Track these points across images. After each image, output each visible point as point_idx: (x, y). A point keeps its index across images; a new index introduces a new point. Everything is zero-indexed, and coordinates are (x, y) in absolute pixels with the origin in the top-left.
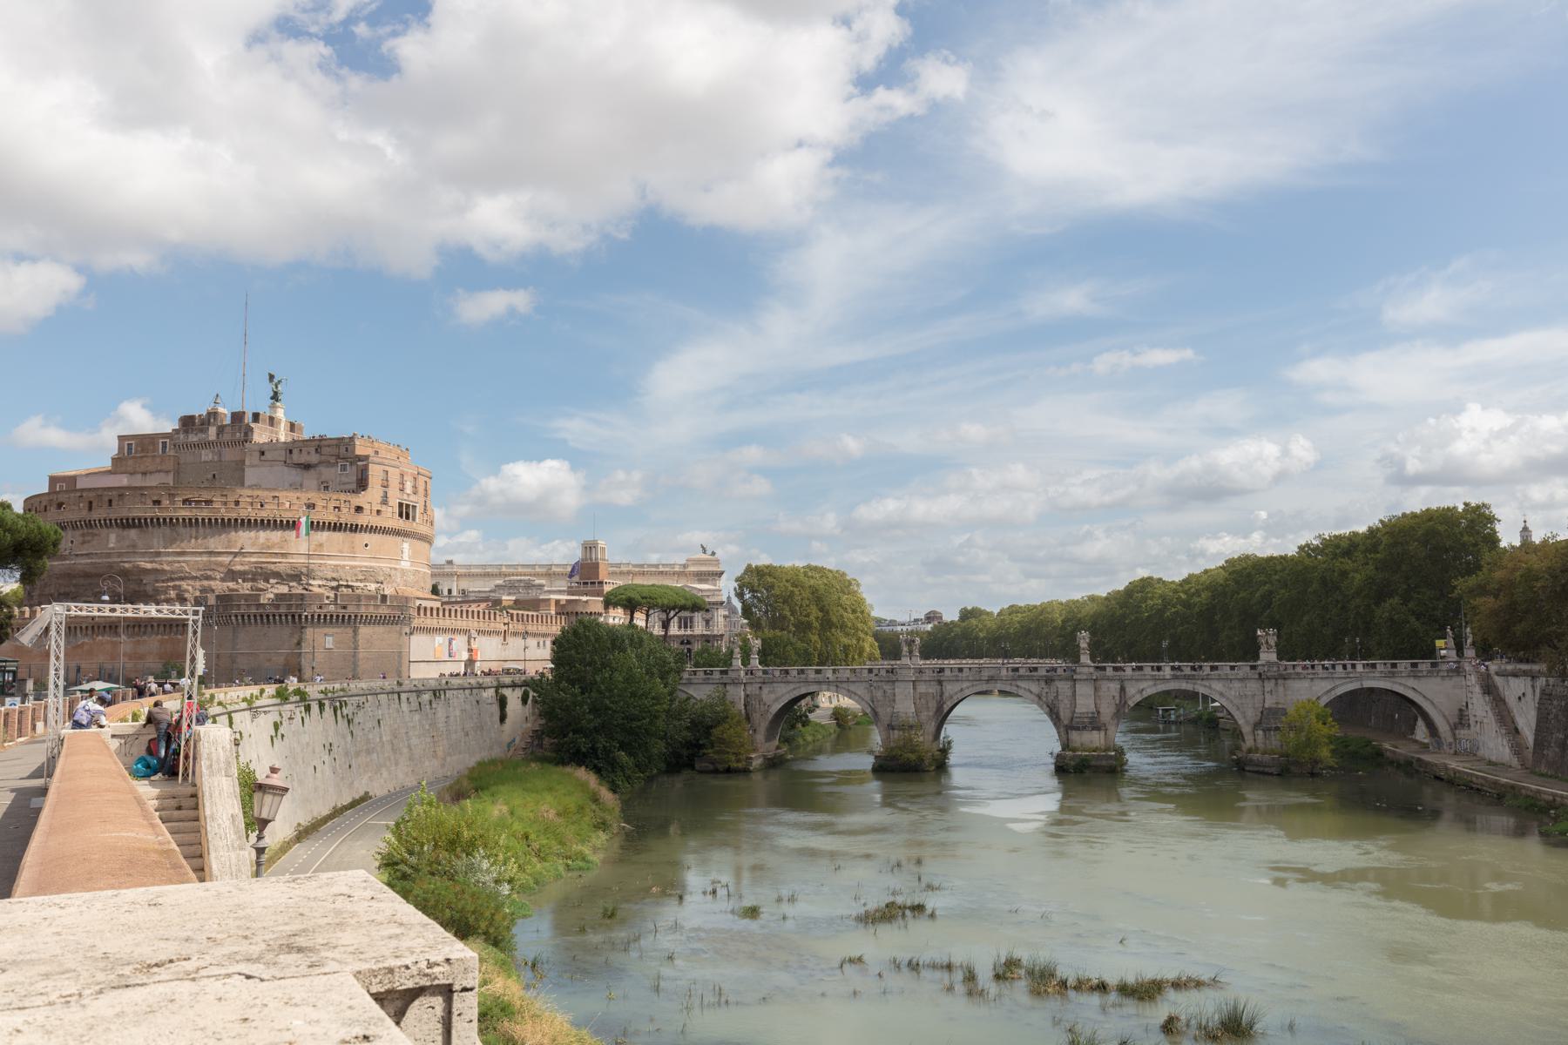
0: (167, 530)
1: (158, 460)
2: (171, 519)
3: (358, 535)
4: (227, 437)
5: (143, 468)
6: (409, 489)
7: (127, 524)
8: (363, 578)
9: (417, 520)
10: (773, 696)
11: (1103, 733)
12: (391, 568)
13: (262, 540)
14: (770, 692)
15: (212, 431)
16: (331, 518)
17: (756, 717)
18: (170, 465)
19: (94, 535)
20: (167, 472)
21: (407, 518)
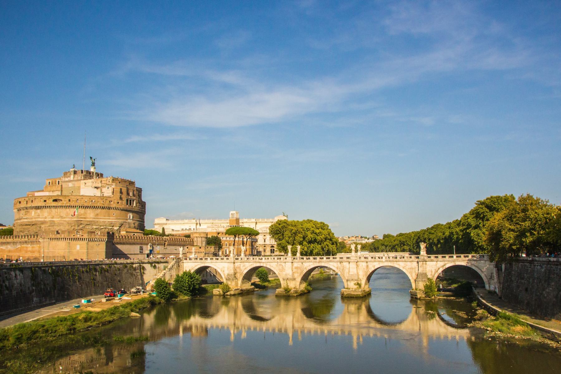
0: (48, 210)
3: (111, 211)
5: (52, 190)
6: (131, 194)
7: (37, 208)
8: (113, 225)
10: (244, 267)
12: (124, 222)
14: (243, 266)
15: (72, 176)
17: (238, 275)
18: (60, 189)
19: (28, 212)
20: (59, 191)
21: (130, 204)
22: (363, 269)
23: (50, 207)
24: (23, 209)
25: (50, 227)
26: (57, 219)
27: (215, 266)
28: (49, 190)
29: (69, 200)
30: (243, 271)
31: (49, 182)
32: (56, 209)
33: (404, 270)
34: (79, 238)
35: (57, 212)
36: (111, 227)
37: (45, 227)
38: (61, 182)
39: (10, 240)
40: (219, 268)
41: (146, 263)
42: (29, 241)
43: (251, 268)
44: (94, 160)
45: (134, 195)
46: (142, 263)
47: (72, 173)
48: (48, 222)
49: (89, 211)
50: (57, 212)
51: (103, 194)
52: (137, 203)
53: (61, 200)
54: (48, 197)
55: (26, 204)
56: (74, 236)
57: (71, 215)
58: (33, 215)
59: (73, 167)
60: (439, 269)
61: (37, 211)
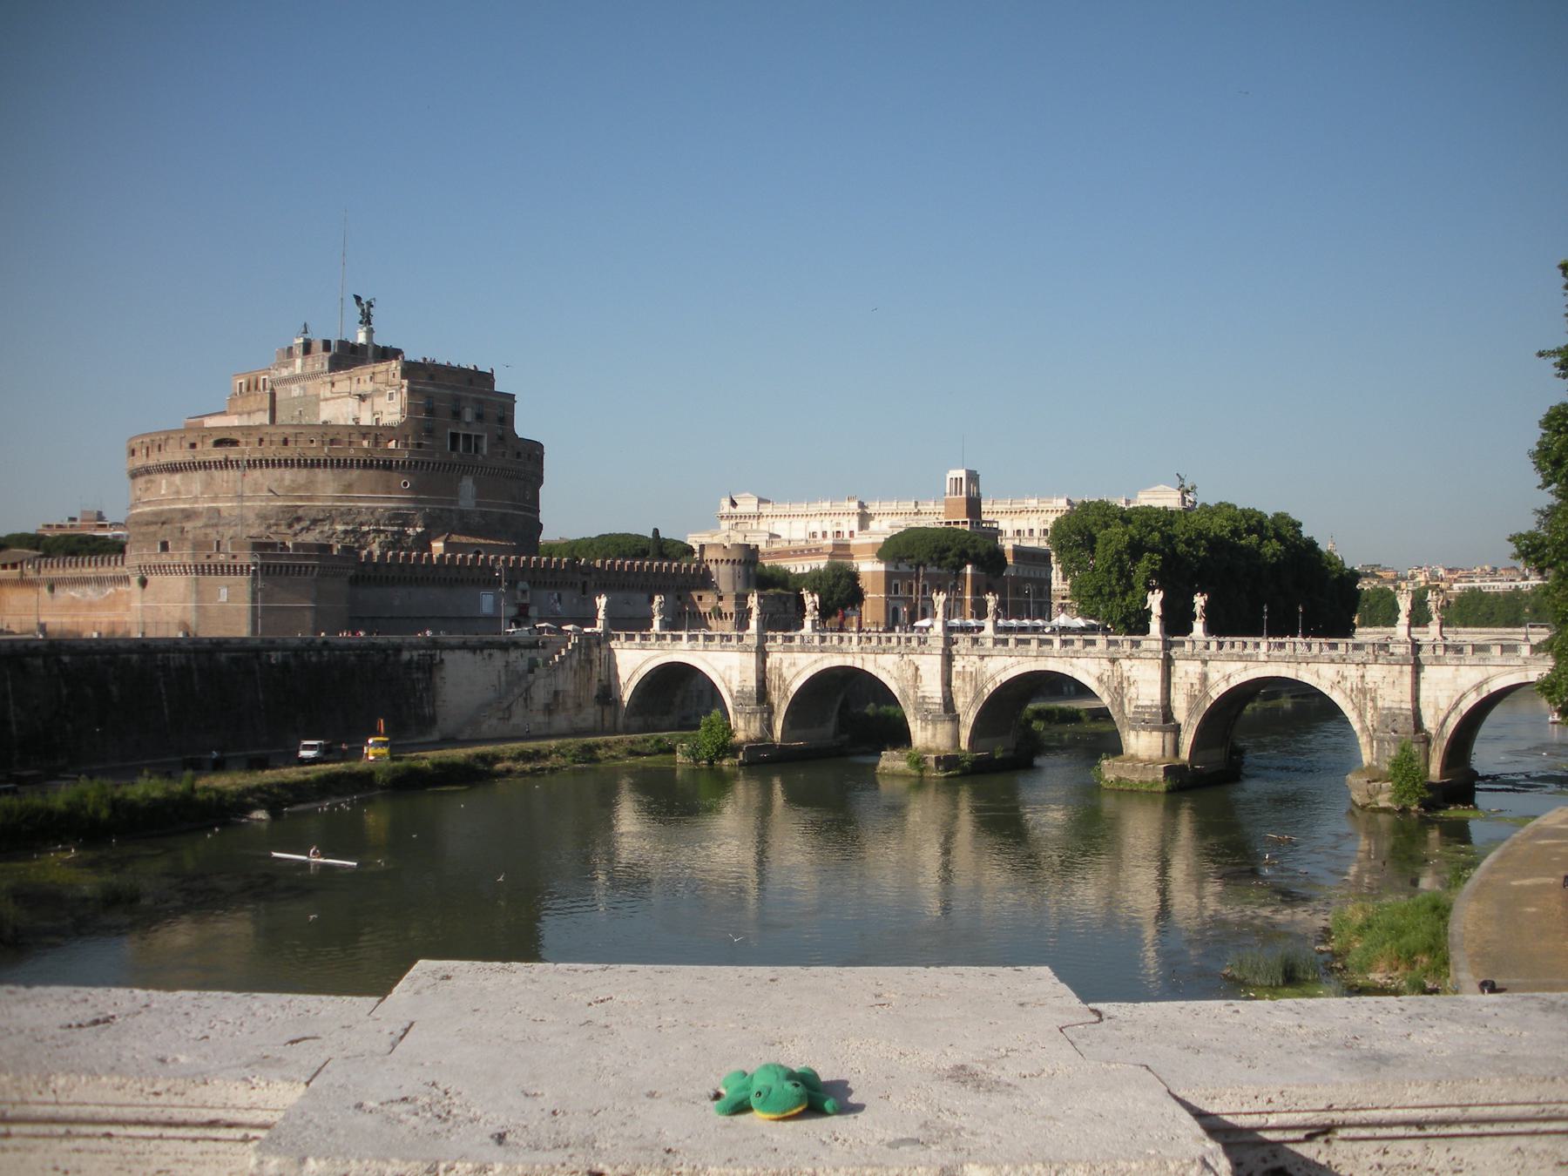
0: (200, 475)
1: (259, 398)
2: (204, 463)
3: (395, 475)
5: (248, 409)
6: (468, 415)
7: (174, 468)
9: (485, 451)
10: (794, 670)
11: (1169, 737)
12: (442, 510)
13: (287, 482)
14: (790, 664)
15: (299, 362)
17: (775, 697)
18: (266, 404)
19: (151, 481)
20: (265, 411)
21: (468, 449)
22: (1189, 687)
23: (205, 466)
24: (142, 475)
25: (209, 531)
26: (227, 502)
27: (704, 660)
28: (239, 410)
29: (261, 441)
30: (791, 683)
31: (241, 384)
32: (225, 472)
33: (1337, 697)
35: (227, 482)
36: (396, 528)
40: (715, 670)
41: (452, 648)
43: (815, 672)
44: (370, 305)
45: (479, 417)
46: (436, 649)
47: (298, 351)
48: (202, 513)
49: (321, 474)
51: (377, 416)
52: (491, 445)
53: (234, 443)
54: (201, 434)
56: (209, 557)
57: (265, 488)
58: (163, 492)
59: (303, 329)
60: (1463, 696)
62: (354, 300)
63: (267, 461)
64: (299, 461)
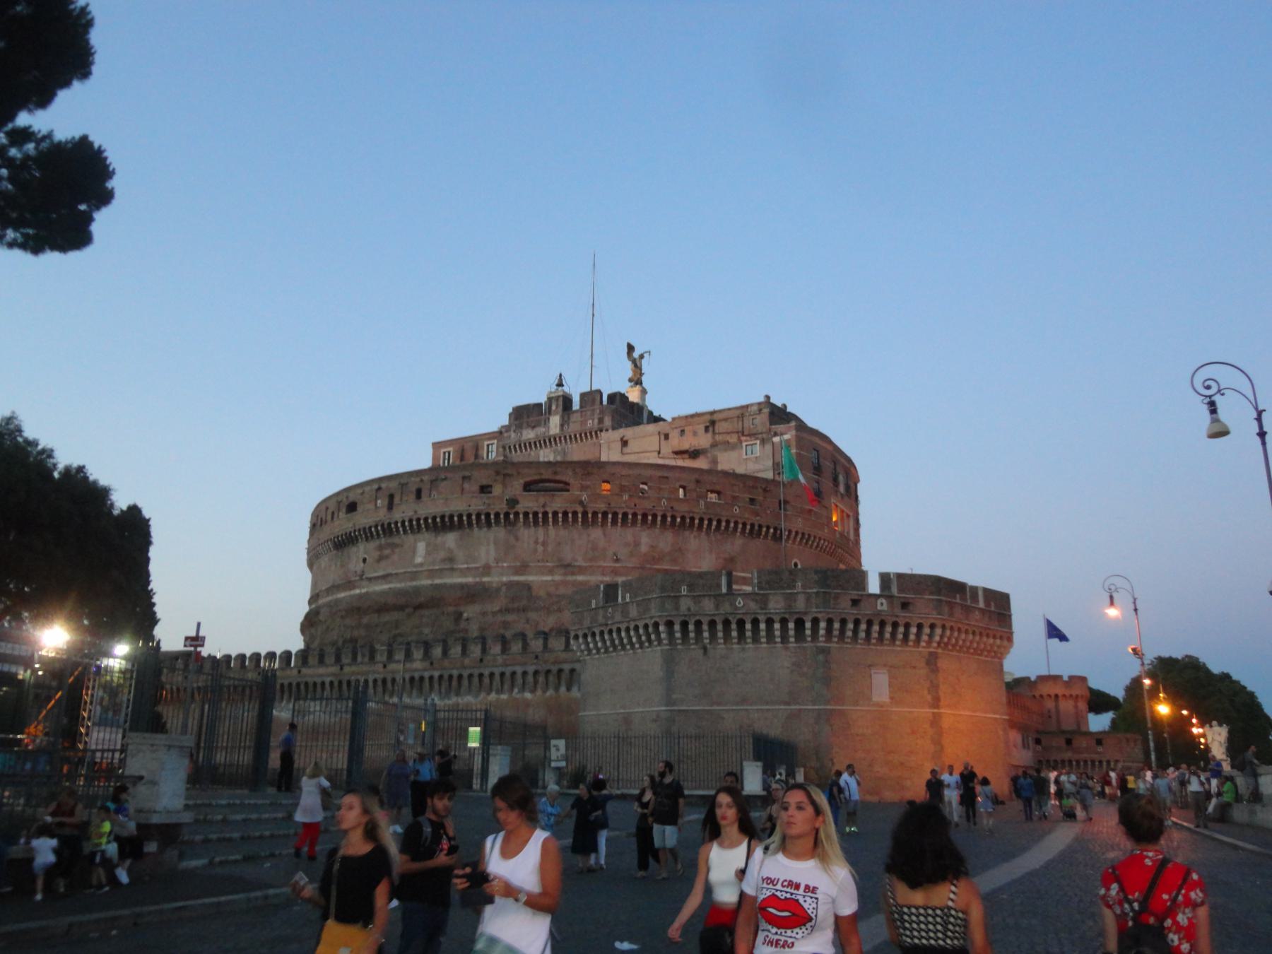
0: (499, 532)
4: (574, 427)
7: (444, 524)
13: (644, 548)
15: (555, 421)
16: (747, 516)
23: (508, 518)
25: (510, 618)
26: (543, 574)
32: (541, 531)
34: (890, 620)
35: (544, 544)
37: (484, 614)
38: (504, 448)
39: (322, 670)
42: (436, 674)
44: (642, 357)
48: (498, 590)
49: (694, 541)
50: (544, 544)
55: (385, 510)
57: (610, 553)
58: (419, 560)
61: (439, 539)
62: (626, 350)
63: (615, 514)
64: (664, 517)
